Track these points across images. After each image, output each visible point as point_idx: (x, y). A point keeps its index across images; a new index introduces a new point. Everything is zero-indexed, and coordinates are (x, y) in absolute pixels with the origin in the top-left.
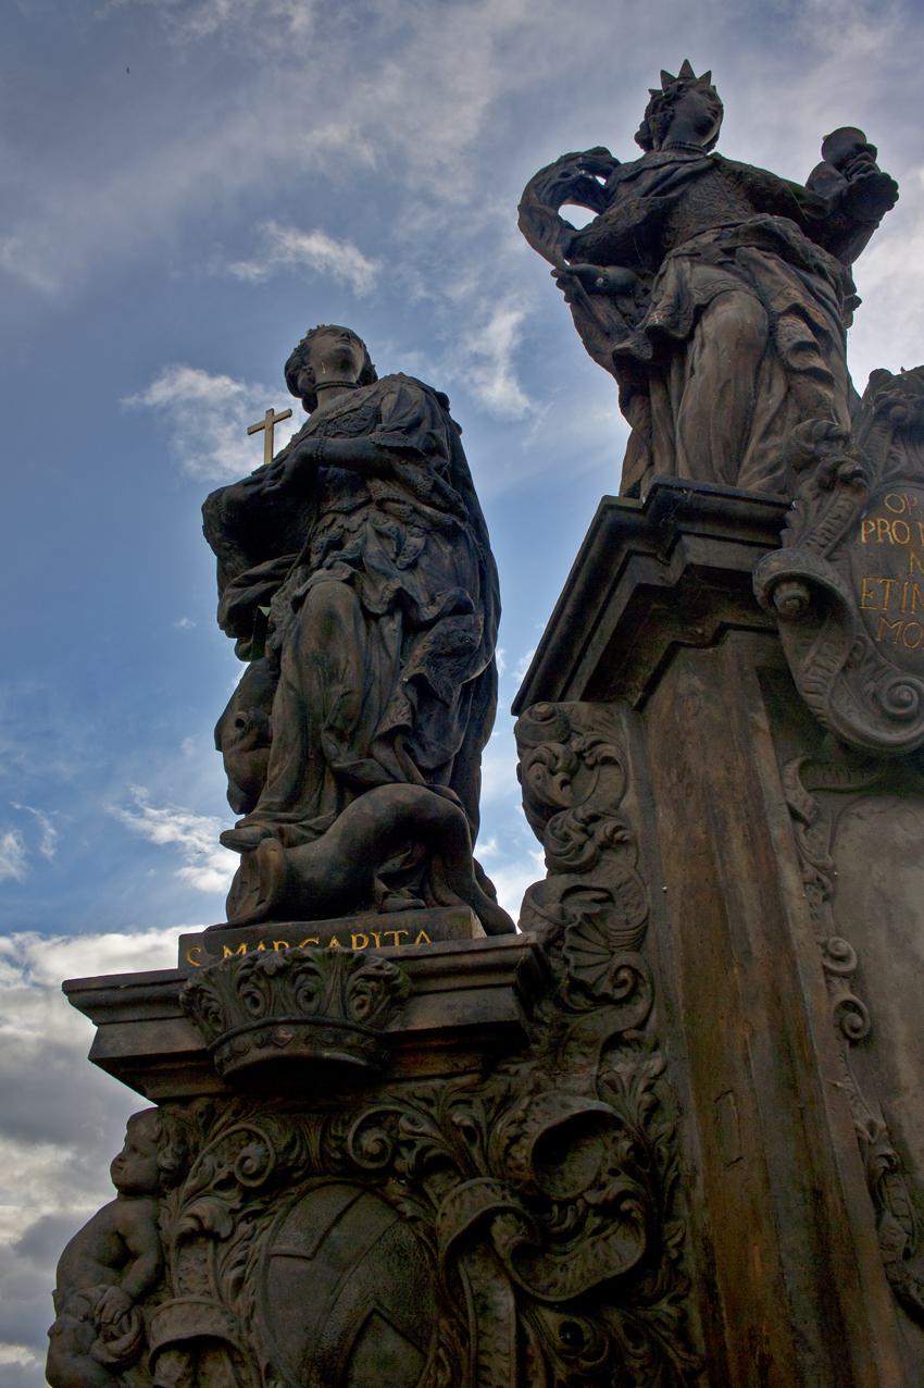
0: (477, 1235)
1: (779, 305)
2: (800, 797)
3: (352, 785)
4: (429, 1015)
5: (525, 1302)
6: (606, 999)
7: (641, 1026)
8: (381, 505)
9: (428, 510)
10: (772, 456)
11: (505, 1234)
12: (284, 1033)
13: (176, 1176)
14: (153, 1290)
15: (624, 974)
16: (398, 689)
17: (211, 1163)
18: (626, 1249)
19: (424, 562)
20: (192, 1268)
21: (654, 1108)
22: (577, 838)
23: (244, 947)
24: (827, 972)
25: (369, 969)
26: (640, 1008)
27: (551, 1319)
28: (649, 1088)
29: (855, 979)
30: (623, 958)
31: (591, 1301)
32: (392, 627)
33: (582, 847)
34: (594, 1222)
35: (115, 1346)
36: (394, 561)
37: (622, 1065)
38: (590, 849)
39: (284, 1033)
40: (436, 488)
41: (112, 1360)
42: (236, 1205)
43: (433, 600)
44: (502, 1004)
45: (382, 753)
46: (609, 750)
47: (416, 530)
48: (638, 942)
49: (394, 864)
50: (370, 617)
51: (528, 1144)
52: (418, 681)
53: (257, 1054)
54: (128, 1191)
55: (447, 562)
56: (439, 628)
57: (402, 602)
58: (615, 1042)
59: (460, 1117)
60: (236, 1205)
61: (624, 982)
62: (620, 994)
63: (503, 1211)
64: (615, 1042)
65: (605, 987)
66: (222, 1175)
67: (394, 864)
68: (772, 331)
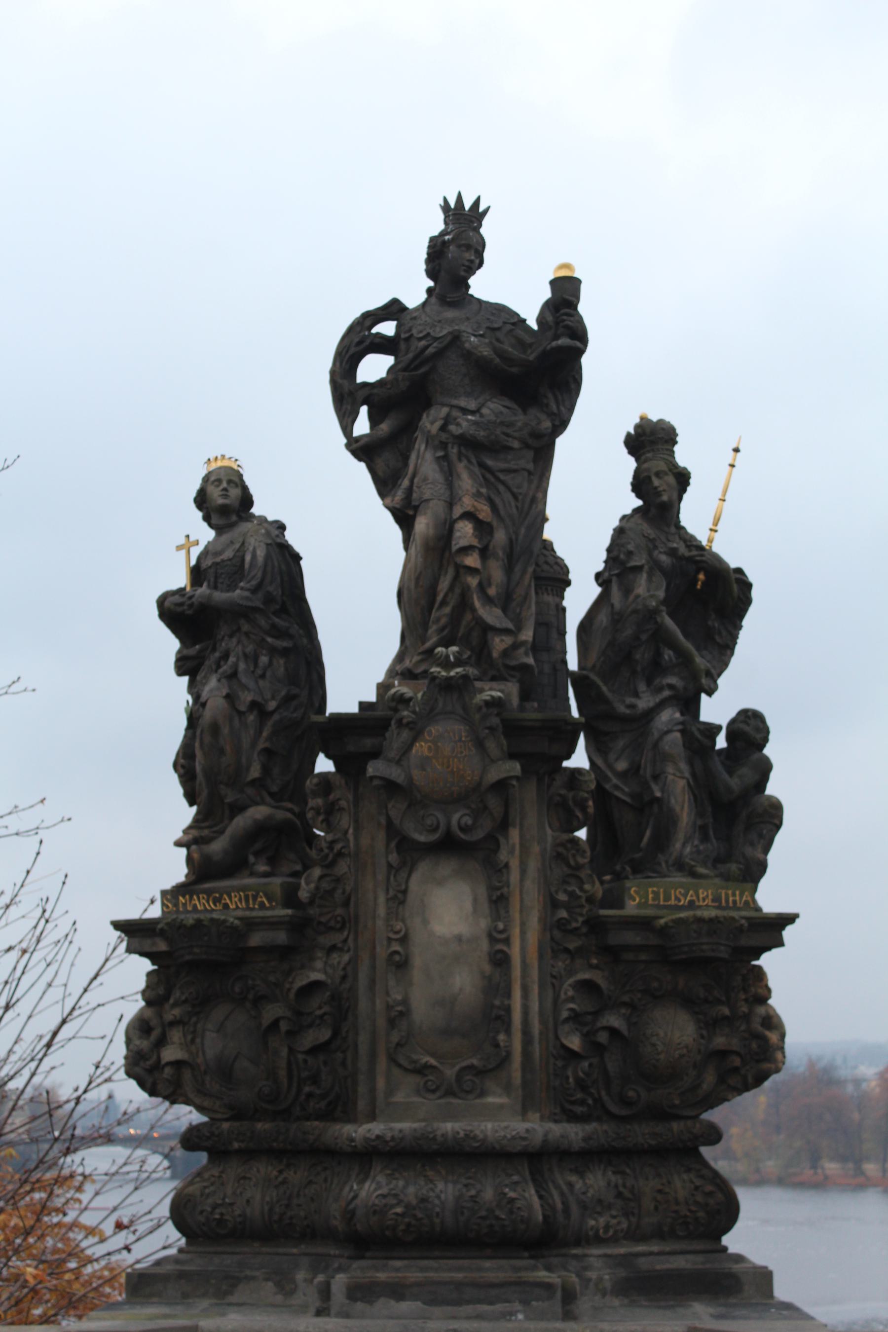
0: (275, 1024)
1: (458, 511)
2: (394, 858)
3: (237, 809)
4: (256, 940)
5: (291, 1050)
6: (331, 929)
7: (345, 941)
8: (247, 634)
9: (269, 640)
10: (444, 621)
11: (284, 1026)
12: (196, 950)
13: (166, 998)
14: (161, 1042)
15: (339, 919)
16: (255, 756)
17: (177, 994)
18: (325, 1034)
19: (268, 674)
20: (176, 1035)
21: (344, 977)
22: (326, 851)
23: (187, 897)
24: (390, 940)
25: (228, 924)
26: (346, 933)
27: (301, 1057)
28: (344, 969)
29: (404, 940)
30: (339, 911)
31: (314, 1050)
32: (251, 718)
33: (327, 856)
34: (318, 1022)
35: (148, 1063)
36: (253, 672)
37: (335, 957)
38: (331, 856)
39: (196, 950)
40: (274, 626)
41: (148, 1067)
42: (190, 1009)
43: (273, 698)
44: (281, 937)
45: (250, 791)
46: (343, 803)
47: (264, 652)
48: (346, 904)
49: (258, 846)
50: (241, 714)
51: (293, 991)
52: (267, 752)
53: (188, 958)
54: (149, 1002)
55: (282, 669)
56: (276, 717)
57: (254, 705)
58: (333, 948)
59: (272, 978)
60: (190, 1009)
61: (338, 922)
62: (338, 926)
63: (283, 1018)
64: (333, 948)
65: (332, 923)
66: (183, 998)
67: (258, 846)
68: (451, 531)
